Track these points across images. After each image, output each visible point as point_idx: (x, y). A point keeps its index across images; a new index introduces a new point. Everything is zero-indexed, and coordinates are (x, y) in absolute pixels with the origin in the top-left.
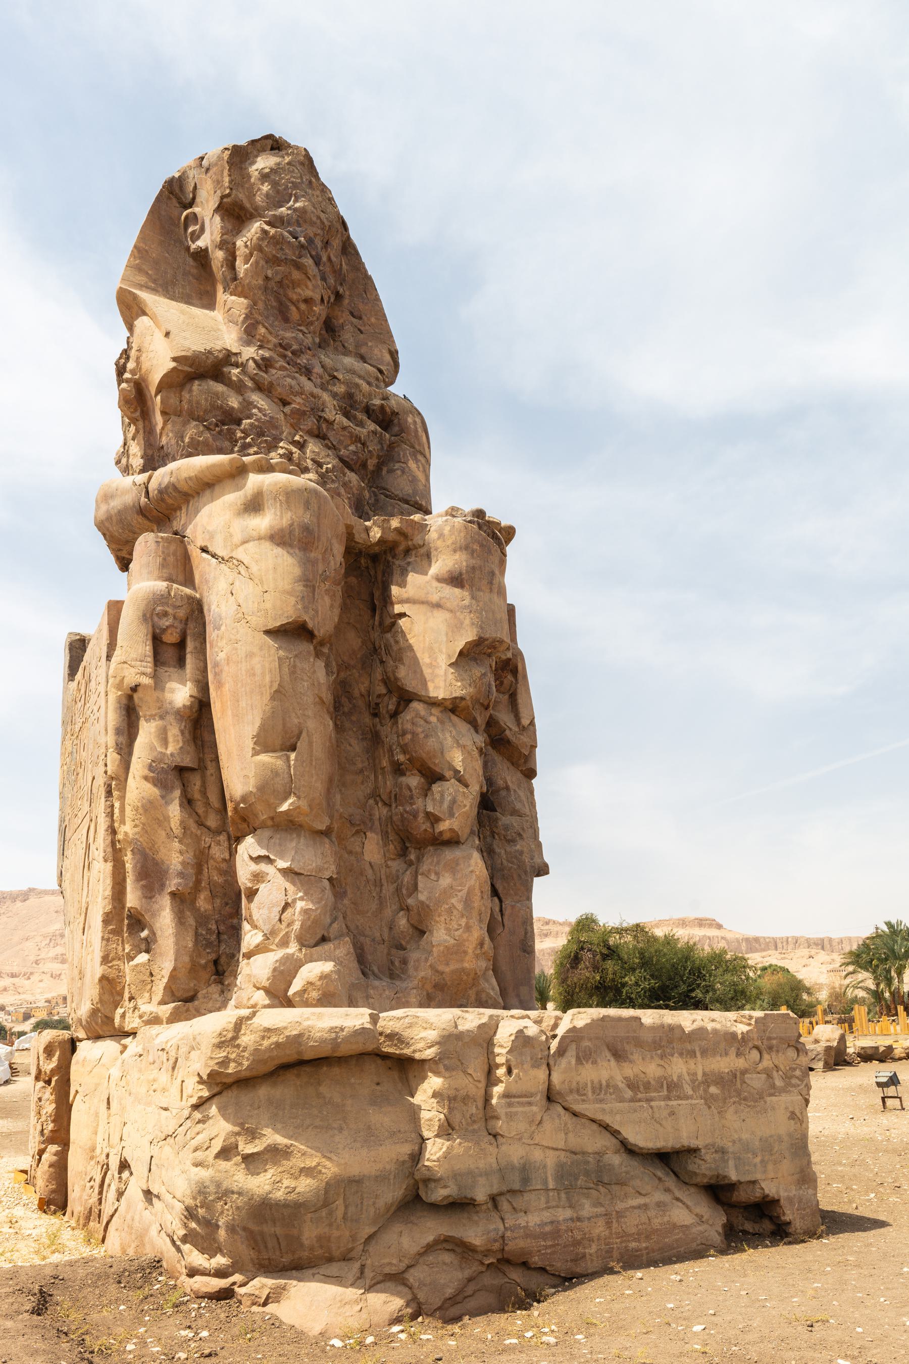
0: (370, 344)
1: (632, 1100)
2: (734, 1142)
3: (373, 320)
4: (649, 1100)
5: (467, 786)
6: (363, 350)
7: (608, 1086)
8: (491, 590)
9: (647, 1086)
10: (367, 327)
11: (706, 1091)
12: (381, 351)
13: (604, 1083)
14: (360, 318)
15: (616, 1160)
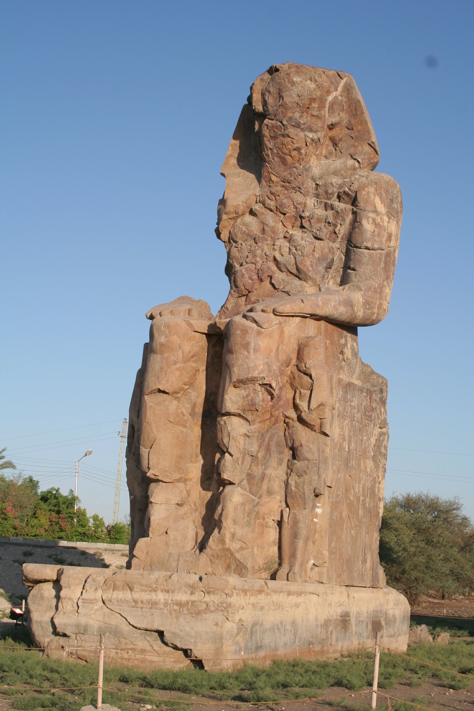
0: (356, 144)
1: (133, 607)
2: (181, 631)
3: (359, 127)
4: (141, 608)
5: (232, 456)
6: (352, 150)
7: (125, 600)
8: (248, 352)
9: (142, 602)
10: (356, 133)
11: (170, 607)
12: (362, 146)
13: (123, 599)
14: (352, 129)
15: (126, 628)
